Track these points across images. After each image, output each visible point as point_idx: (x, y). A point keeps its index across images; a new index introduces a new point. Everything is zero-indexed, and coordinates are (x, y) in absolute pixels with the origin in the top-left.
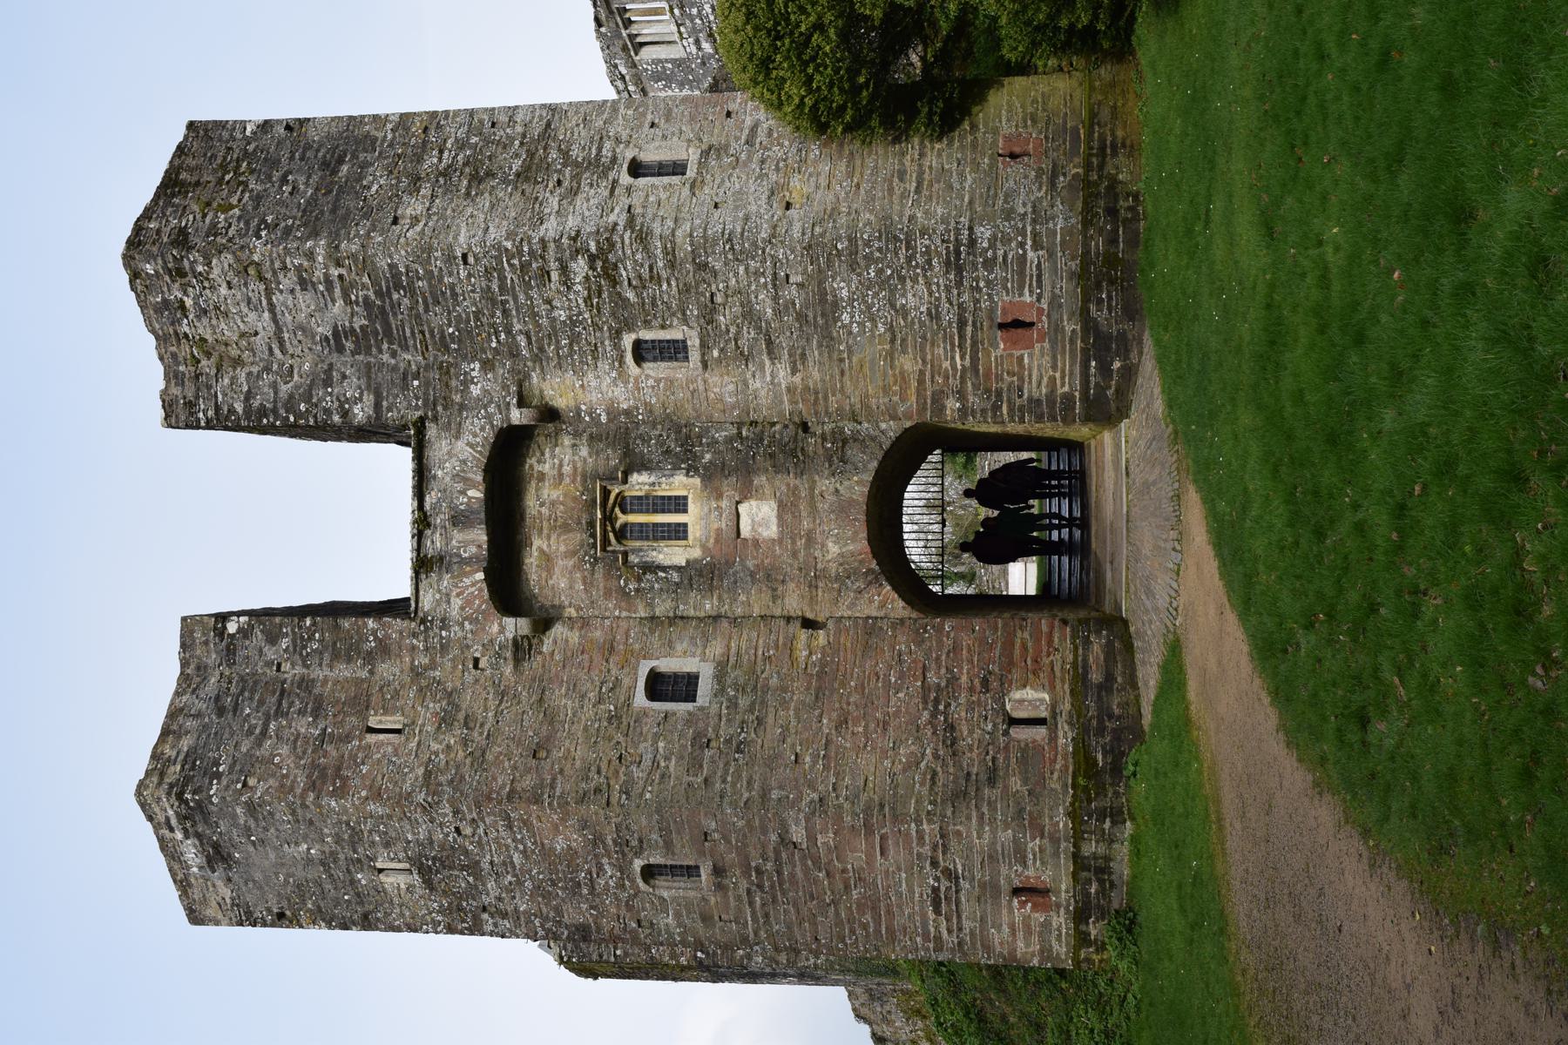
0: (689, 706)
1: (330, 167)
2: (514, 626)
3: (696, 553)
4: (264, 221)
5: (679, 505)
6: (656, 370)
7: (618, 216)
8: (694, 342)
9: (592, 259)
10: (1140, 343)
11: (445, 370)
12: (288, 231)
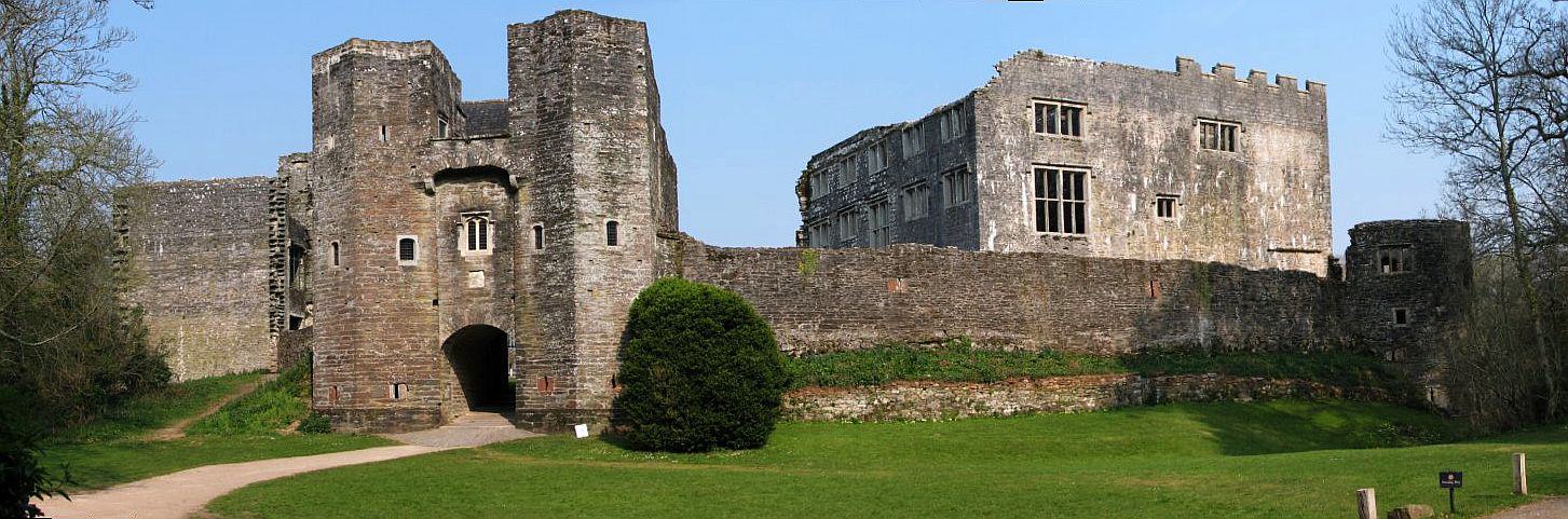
0: (398, 258)
2: (429, 182)
3: (463, 254)
4: (588, 66)
5: (483, 246)
7: (587, 220)
8: (541, 252)
10: (540, 432)
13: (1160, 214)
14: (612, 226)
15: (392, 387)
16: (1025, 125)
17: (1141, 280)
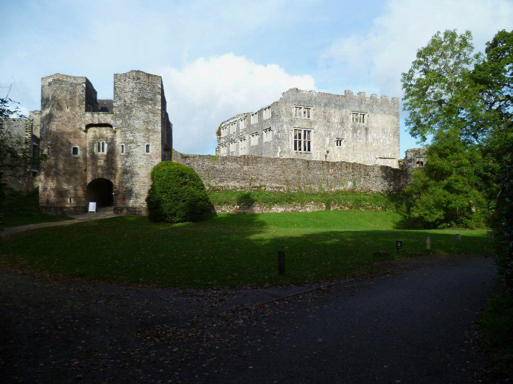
1: (151, 100)
2: (84, 128)
3: (96, 154)
5: (103, 151)
6: (120, 149)
7: (139, 144)
8: (123, 154)
9: (133, 140)
11: (120, 117)
12: (139, 95)
13: (337, 145)
14: (148, 146)
16: (291, 114)
17: (328, 168)
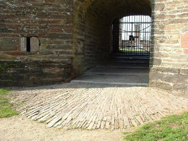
15: (23, 40)
